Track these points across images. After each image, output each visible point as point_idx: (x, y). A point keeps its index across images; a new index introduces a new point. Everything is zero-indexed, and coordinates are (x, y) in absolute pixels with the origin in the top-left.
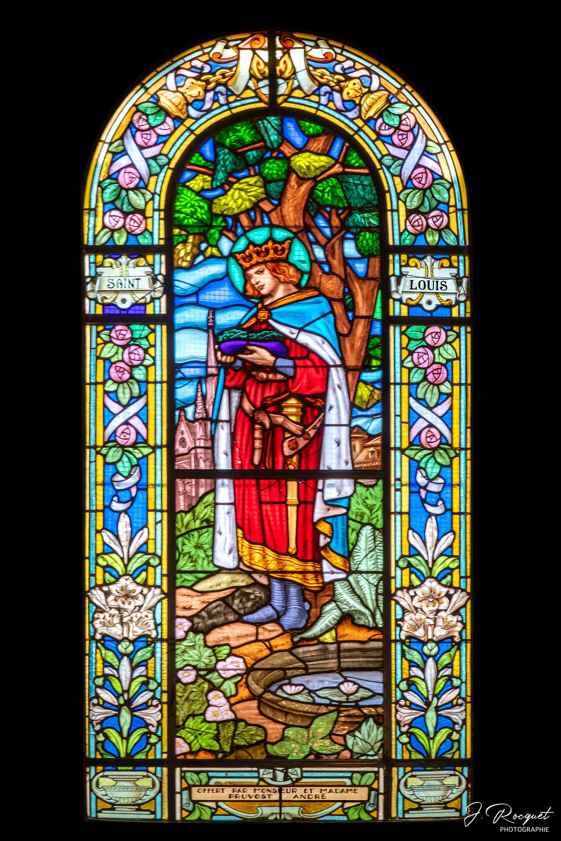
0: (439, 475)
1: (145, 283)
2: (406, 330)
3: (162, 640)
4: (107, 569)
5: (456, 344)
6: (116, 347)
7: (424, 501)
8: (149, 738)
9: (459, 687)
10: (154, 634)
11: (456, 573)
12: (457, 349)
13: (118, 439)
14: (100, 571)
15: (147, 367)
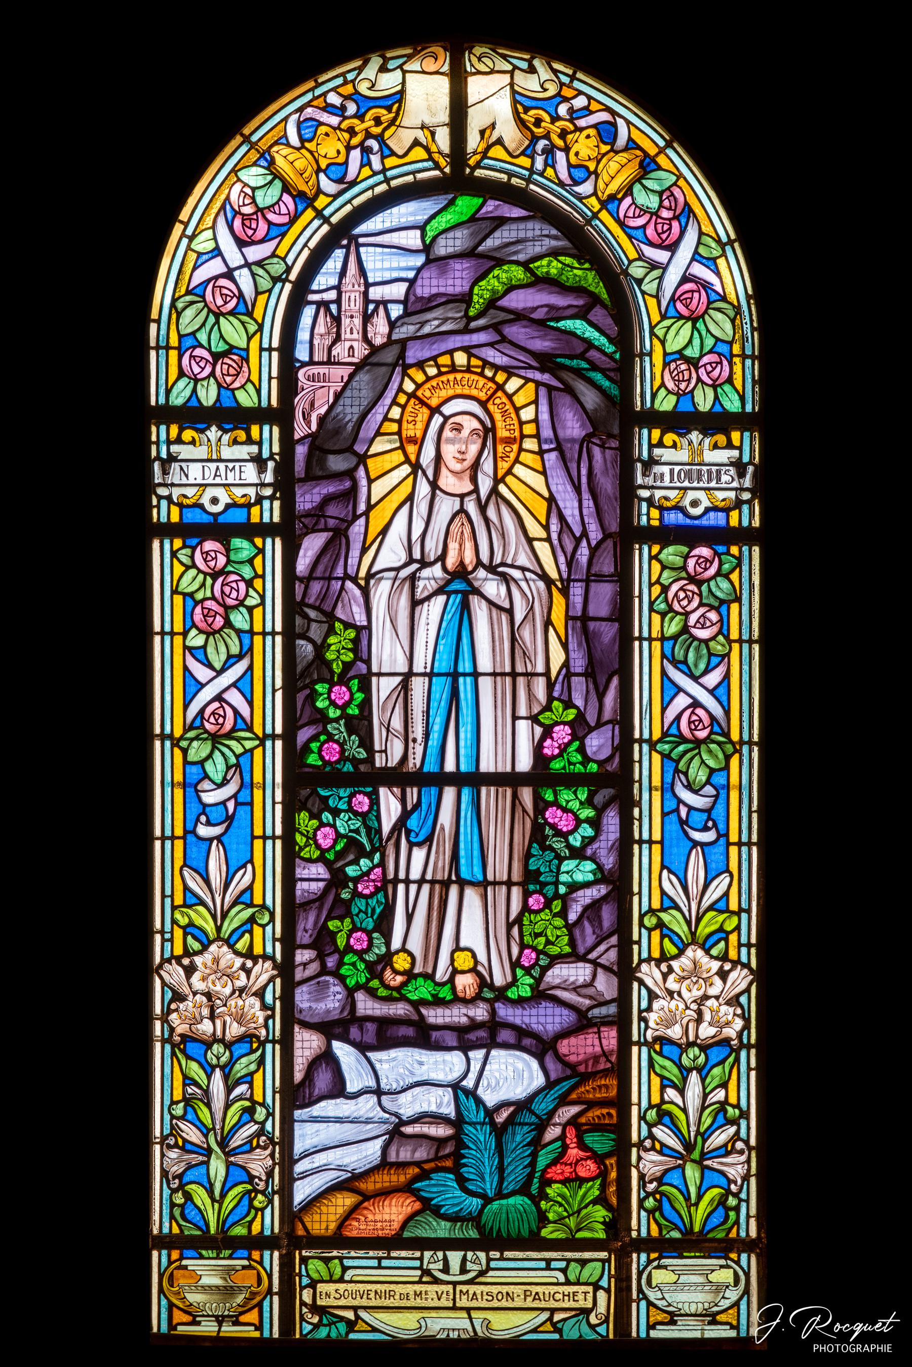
0: (708, 782)
7: (683, 823)
8: (251, 1201)
11: (733, 938)
14: (178, 933)
15: (250, 610)
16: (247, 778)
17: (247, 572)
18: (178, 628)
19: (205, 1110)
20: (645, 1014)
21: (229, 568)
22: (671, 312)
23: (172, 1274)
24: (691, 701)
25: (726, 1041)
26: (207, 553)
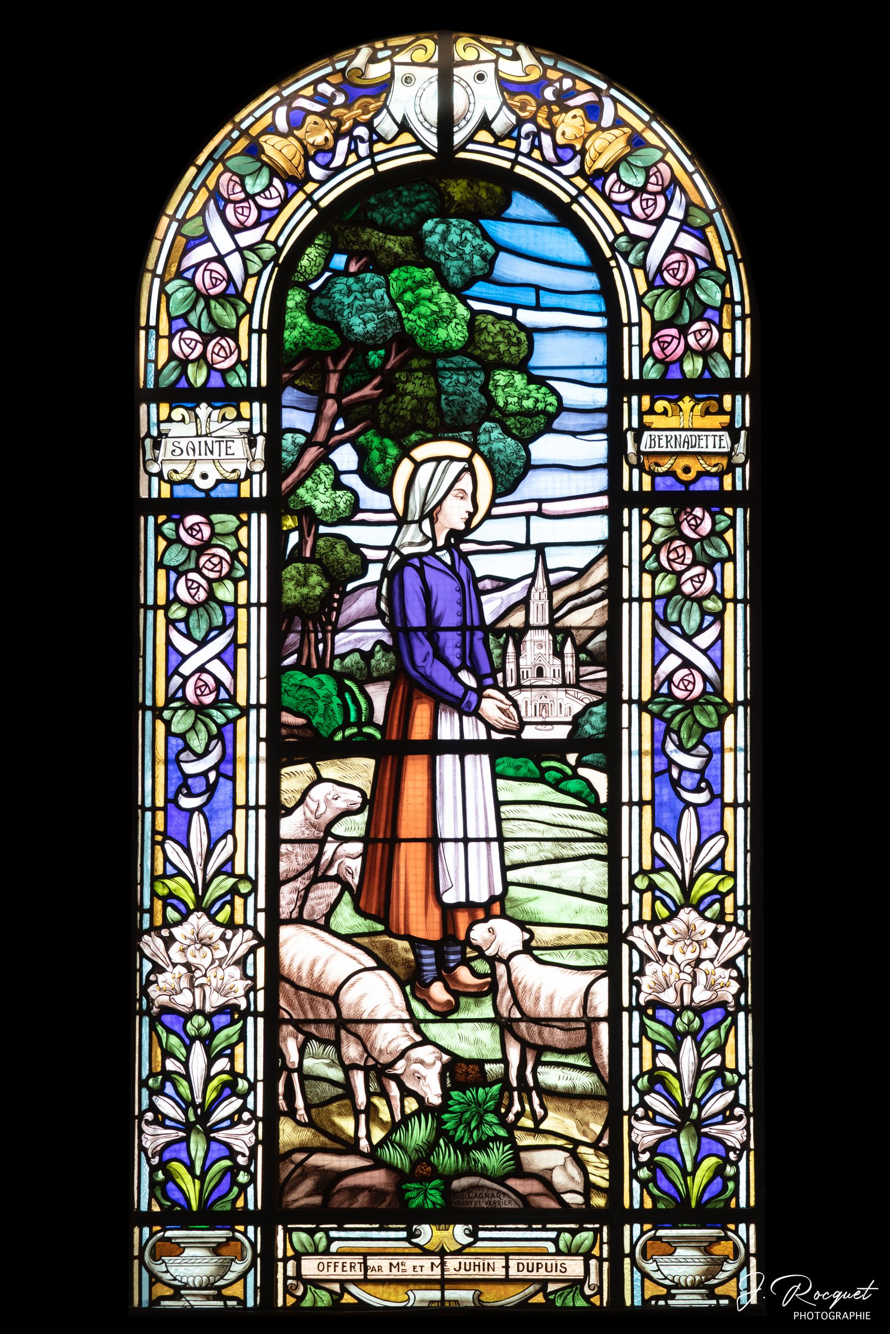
3: (256, 1014)
5: (729, 536)
10: (243, 1004)
11: (729, 901)
16: (229, 750)
18: (162, 601)
19: (185, 1083)
20: (636, 978)
22: (658, 282)
25: (723, 1004)
26: (191, 528)
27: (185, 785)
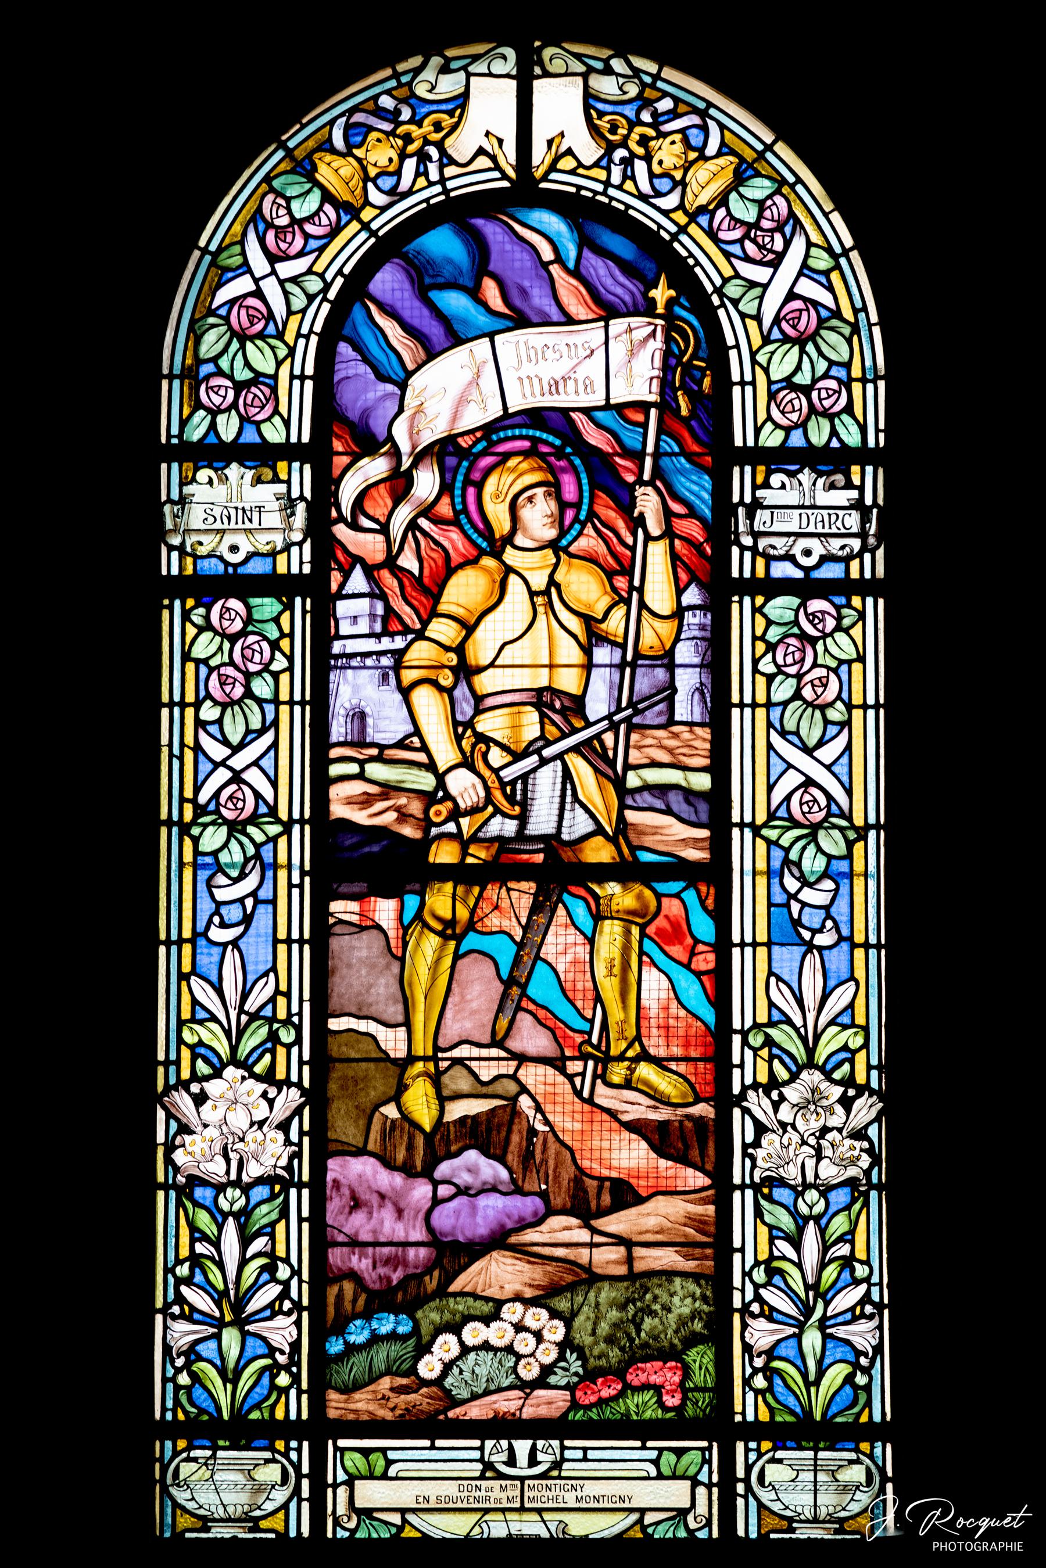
0: (825, 875)
1: (273, 519)
2: (763, 605)
4: (202, 1051)
5: (856, 632)
6: (218, 639)
8: (273, 1377)
9: (867, 1280)
11: (861, 1058)
12: (862, 637)
13: (223, 811)
14: (186, 1054)
15: (276, 676)
17: (273, 633)
18: (190, 698)
20: (750, 1151)
21: (250, 628)
22: (776, 334)
23: (177, 1469)
24: (803, 778)
27: (217, 912)
